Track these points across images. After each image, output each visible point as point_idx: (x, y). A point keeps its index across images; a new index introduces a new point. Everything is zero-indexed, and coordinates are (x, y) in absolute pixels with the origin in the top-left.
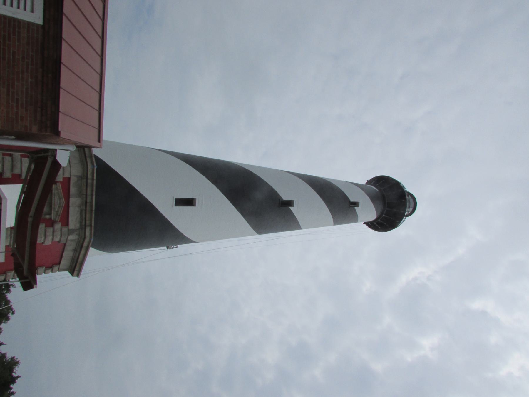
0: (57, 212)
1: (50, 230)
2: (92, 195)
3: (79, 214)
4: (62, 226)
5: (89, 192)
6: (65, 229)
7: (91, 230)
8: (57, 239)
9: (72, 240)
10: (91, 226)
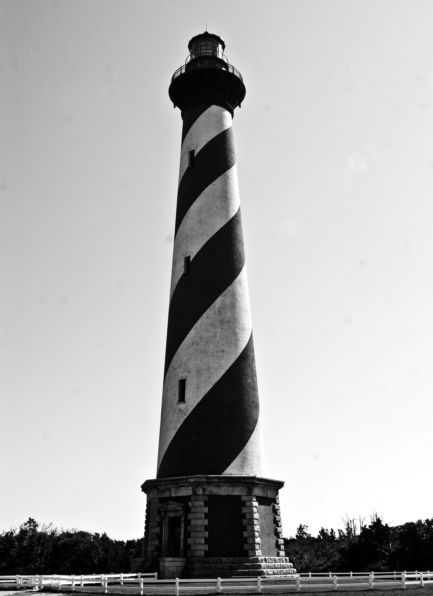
0: (177, 505)
1: (193, 510)
2: (166, 481)
3: (182, 488)
4: (190, 500)
5: (164, 483)
6: (192, 498)
7: (190, 478)
8: (202, 504)
9: (204, 490)
10: (187, 479)
